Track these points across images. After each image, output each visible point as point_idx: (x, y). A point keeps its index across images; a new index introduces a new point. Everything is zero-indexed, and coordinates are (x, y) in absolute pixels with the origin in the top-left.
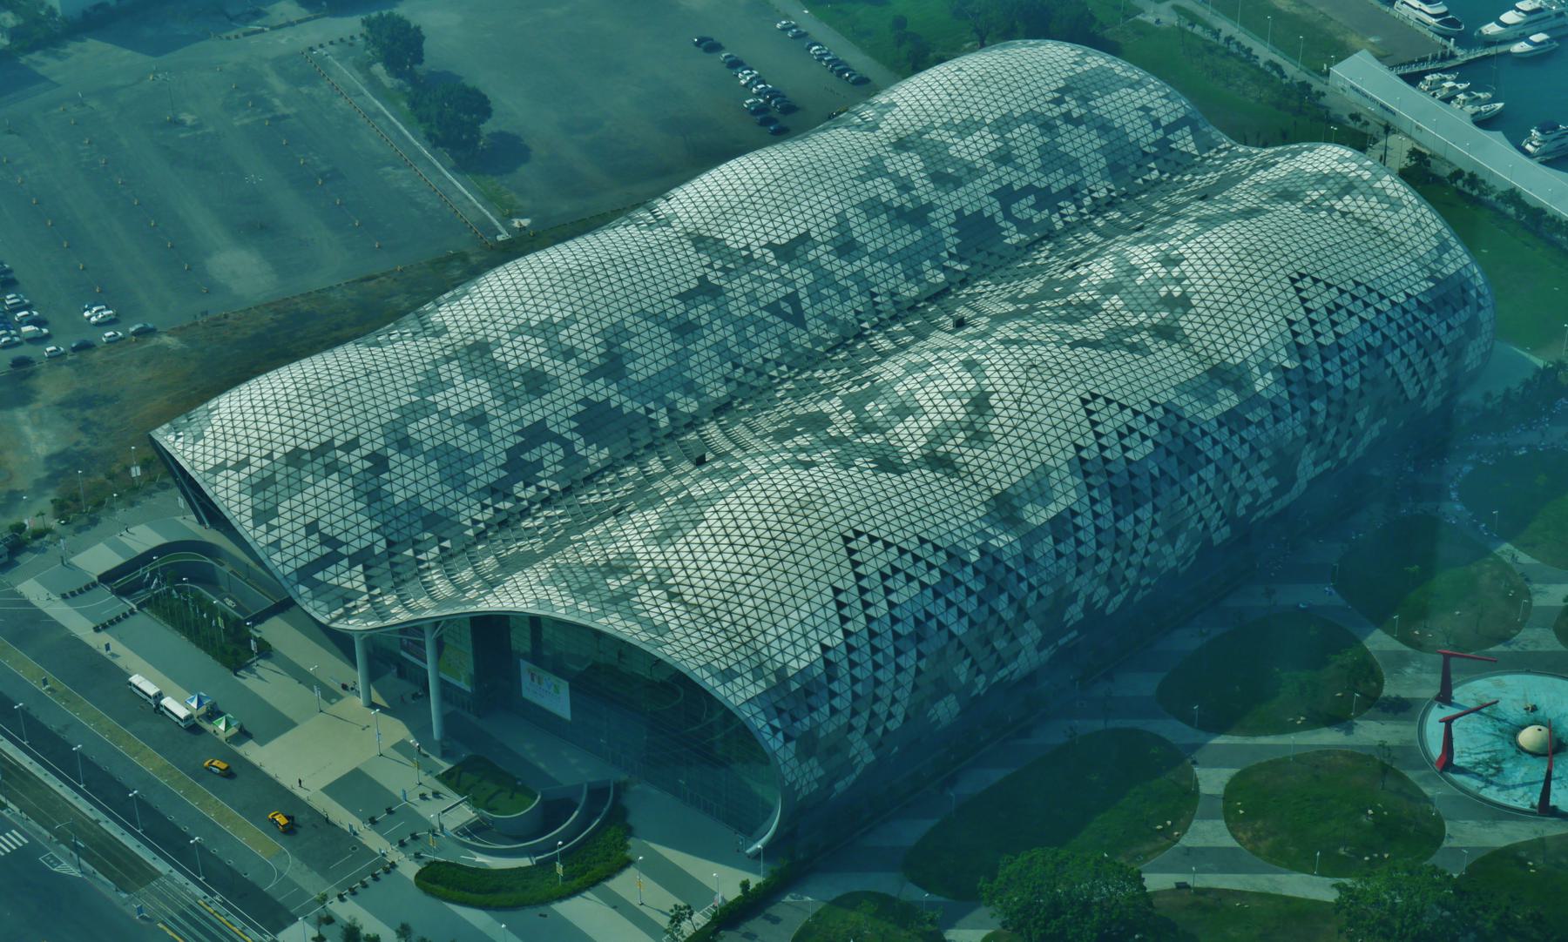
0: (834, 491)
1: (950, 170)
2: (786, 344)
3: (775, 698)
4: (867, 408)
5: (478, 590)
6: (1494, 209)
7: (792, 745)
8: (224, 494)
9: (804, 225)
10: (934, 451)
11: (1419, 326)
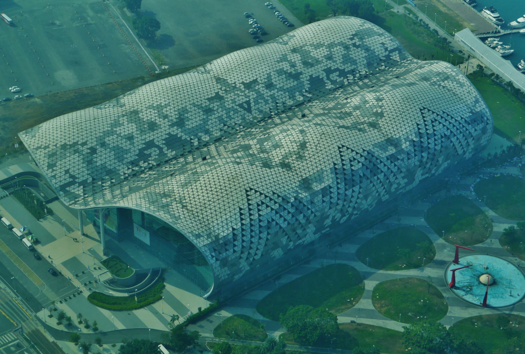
0: (245, 173)
1: (310, 61)
2: (244, 119)
3: (214, 245)
4: (264, 144)
5: (119, 198)
6: (504, 87)
7: (218, 262)
8: (39, 157)
9: (256, 77)
10: (284, 161)
11: (464, 129)
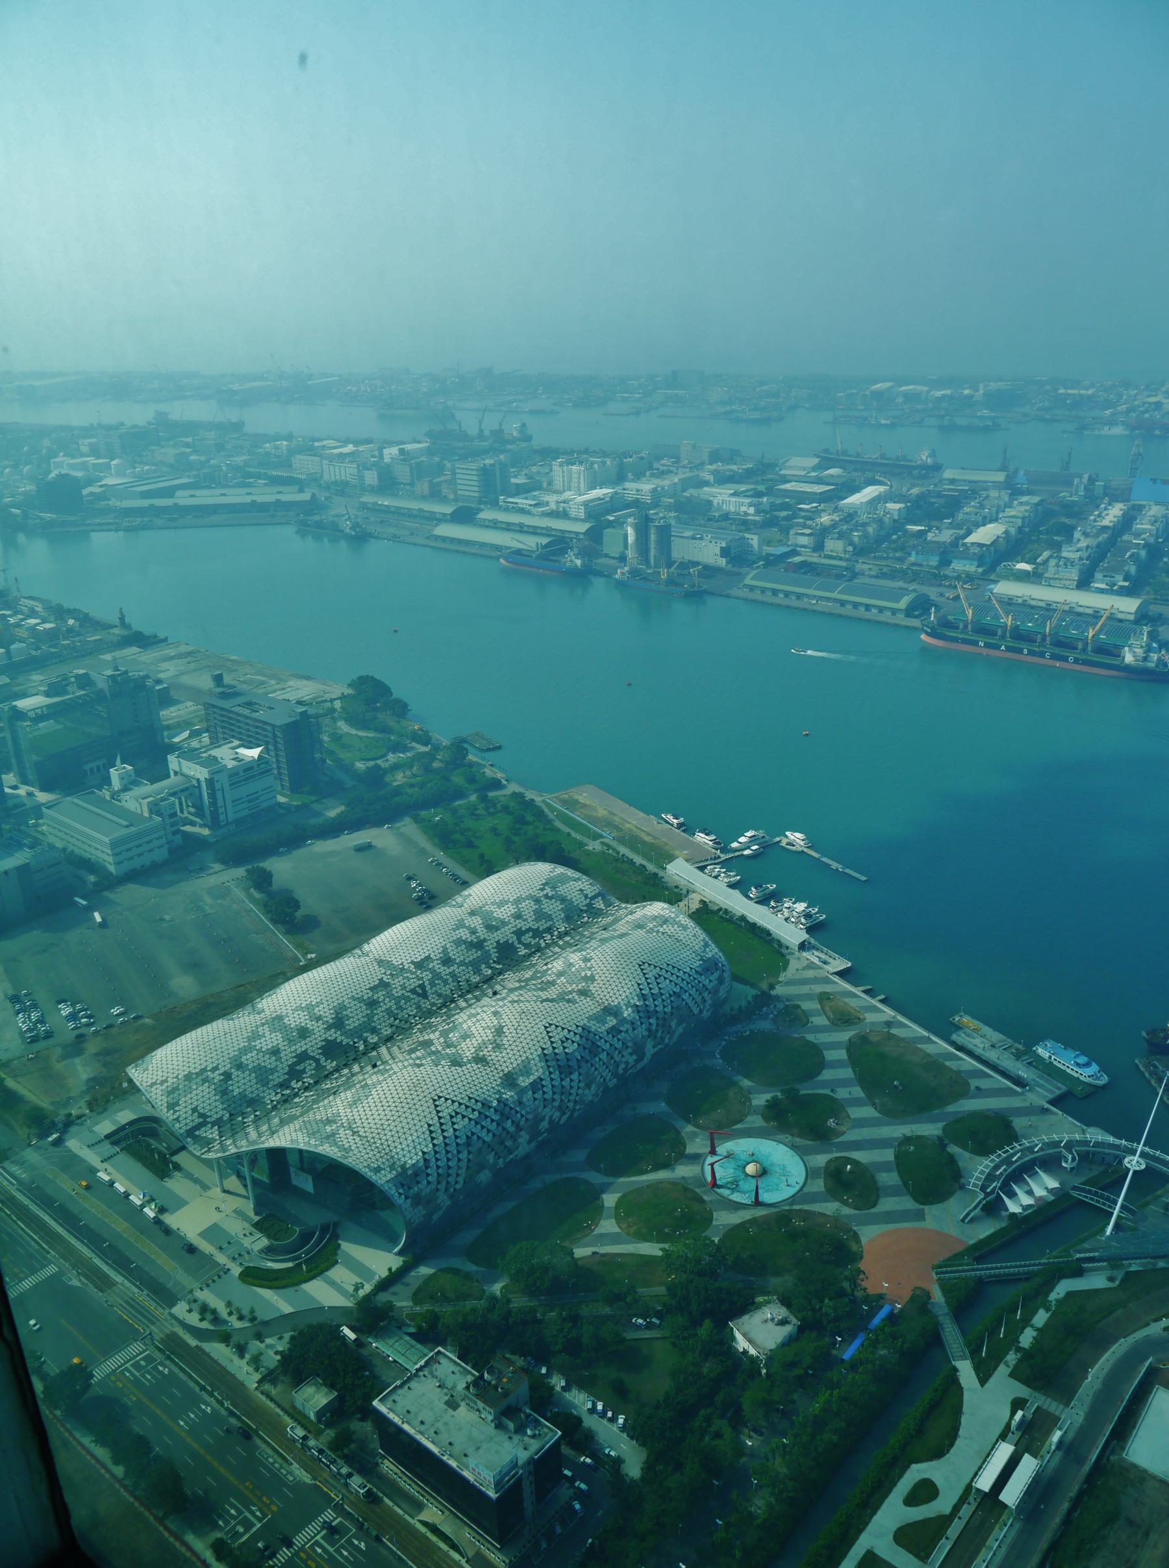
2: (418, 1007)
6: (736, 924)
7: (409, 1201)
